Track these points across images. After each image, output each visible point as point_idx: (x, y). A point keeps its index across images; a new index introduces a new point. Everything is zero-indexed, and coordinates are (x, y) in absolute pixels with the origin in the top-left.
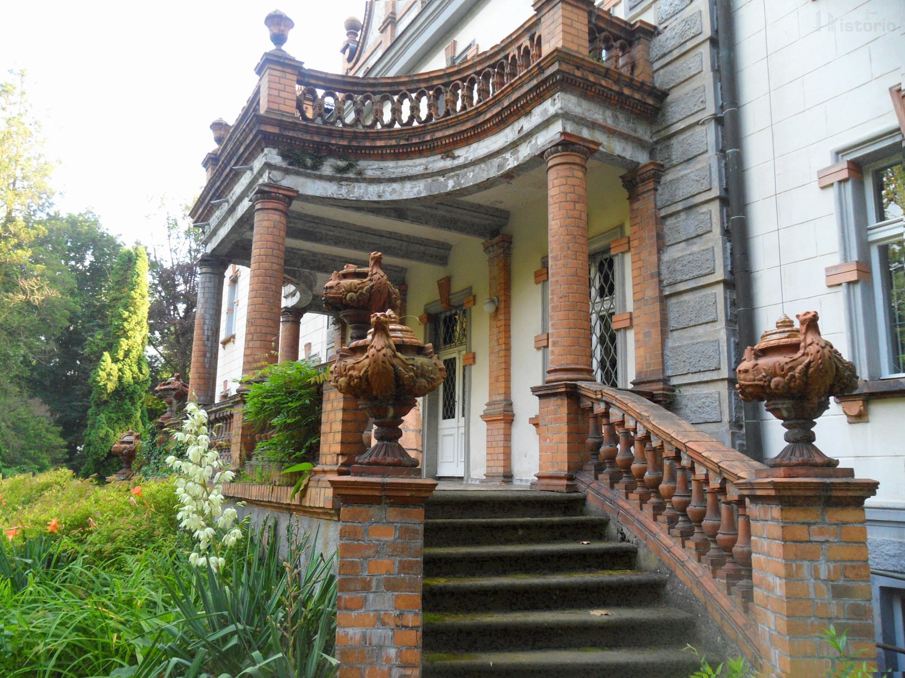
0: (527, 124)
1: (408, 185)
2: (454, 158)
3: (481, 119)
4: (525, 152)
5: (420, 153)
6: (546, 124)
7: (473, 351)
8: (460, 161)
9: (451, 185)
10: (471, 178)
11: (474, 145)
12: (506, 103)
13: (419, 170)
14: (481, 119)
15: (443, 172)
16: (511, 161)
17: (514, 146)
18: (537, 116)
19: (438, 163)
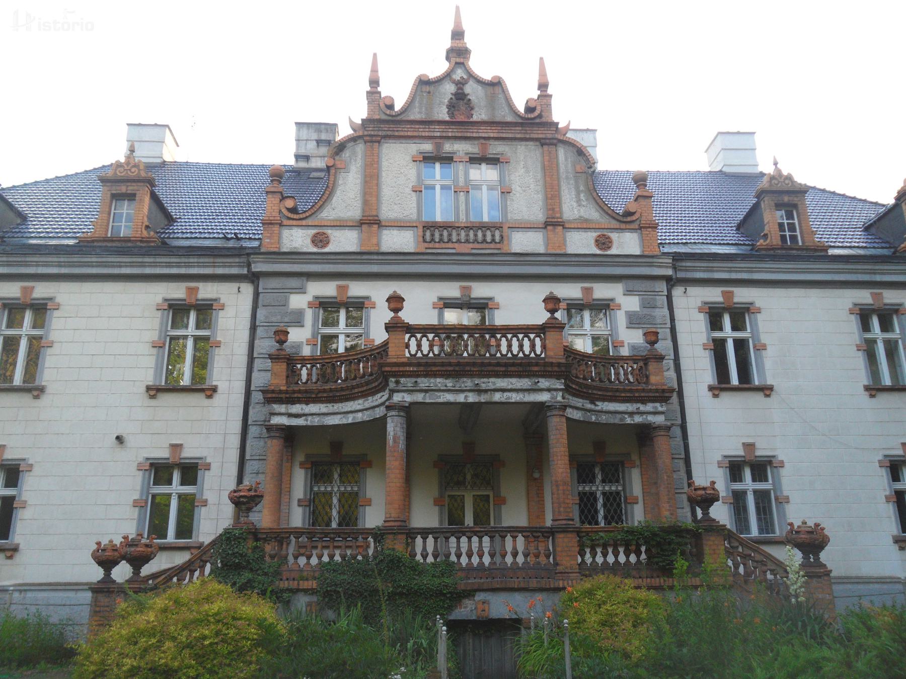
0: (642, 408)
1: (575, 411)
2: (596, 405)
3: (617, 394)
4: (638, 419)
5: (582, 397)
6: (655, 413)
7: (502, 495)
8: (598, 408)
9: (594, 418)
10: (604, 419)
11: (606, 403)
12: (637, 395)
13: (579, 405)
14: (617, 394)
15: (590, 411)
16: (628, 420)
17: (631, 414)
18: (649, 407)
19: (589, 406)
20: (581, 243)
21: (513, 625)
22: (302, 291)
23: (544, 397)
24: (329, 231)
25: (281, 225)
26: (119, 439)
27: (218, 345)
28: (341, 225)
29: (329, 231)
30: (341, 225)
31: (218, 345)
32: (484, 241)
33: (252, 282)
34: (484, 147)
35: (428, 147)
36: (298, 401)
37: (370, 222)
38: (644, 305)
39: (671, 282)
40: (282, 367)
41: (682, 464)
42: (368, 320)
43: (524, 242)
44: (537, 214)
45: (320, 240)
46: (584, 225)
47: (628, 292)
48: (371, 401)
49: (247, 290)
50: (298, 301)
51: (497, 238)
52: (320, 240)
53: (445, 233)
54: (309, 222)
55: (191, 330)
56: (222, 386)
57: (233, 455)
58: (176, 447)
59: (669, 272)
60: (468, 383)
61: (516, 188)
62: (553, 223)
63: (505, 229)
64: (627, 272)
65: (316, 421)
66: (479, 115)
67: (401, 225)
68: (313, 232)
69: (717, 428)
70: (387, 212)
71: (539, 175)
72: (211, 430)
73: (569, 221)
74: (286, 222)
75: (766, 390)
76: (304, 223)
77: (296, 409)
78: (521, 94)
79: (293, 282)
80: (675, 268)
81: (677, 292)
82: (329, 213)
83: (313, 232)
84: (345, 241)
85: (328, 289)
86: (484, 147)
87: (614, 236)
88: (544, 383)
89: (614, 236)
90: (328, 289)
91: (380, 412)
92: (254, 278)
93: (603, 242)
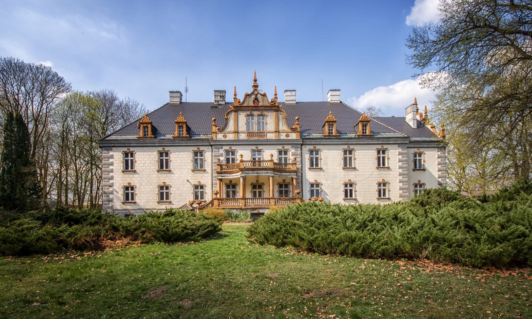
20: (283, 136)
21: (263, 214)
22: (222, 148)
23: (270, 174)
27: (205, 161)
31: (205, 161)
35: (248, 113)
37: (237, 132)
39: (302, 145)
40: (219, 167)
41: (301, 184)
43: (271, 136)
44: (273, 129)
45: (225, 136)
47: (292, 147)
48: (237, 174)
49: (210, 147)
52: (225, 136)
55: (199, 157)
56: (207, 169)
57: (210, 183)
60: (255, 172)
62: (277, 132)
64: (293, 144)
66: (261, 104)
69: (310, 176)
71: (274, 119)
75: (321, 169)
78: (270, 97)
79: (220, 146)
80: (303, 142)
81: (303, 147)
85: (227, 148)
87: (290, 134)
88: (269, 172)
90: (227, 148)
91: (239, 176)
92: (211, 146)
93: (287, 136)
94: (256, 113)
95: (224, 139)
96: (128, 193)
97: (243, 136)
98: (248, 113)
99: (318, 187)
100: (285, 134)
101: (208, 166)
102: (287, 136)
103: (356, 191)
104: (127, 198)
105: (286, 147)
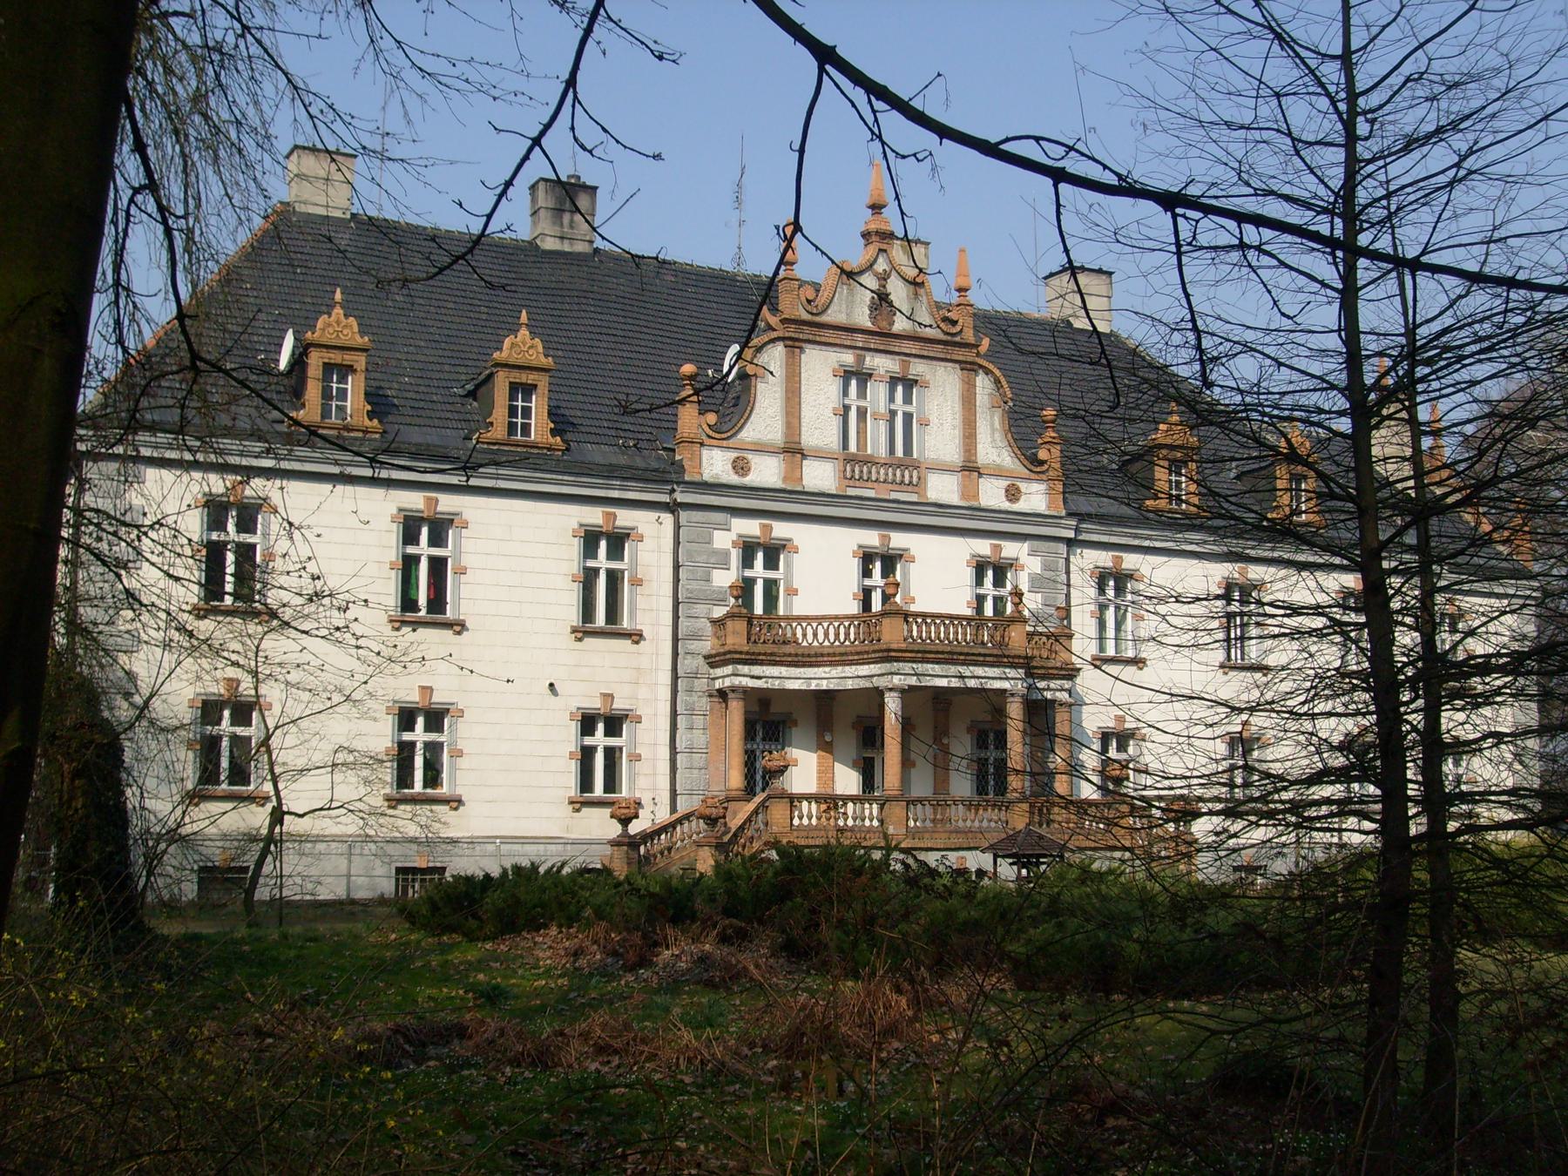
20: (992, 494)
24: (750, 456)
25: (702, 444)
26: (551, 685)
28: (761, 449)
29: (750, 456)
30: (761, 449)
32: (902, 482)
33: (673, 512)
34: (905, 365)
36: (762, 663)
37: (793, 451)
38: (1046, 567)
42: (788, 565)
43: (943, 489)
45: (741, 467)
46: (998, 473)
49: (667, 518)
50: (723, 540)
51: (915, 480)
52: (741, 467)
53: (865, 469)
54: (731, 443)
57: (665, 708)
58: (609, 697)
59: (1071, 534)
61: (933, 419)
63: (923, 470)
65: (777, 684)
67: (821, 455)
68: (734, 455)
69: (1098, 700)
70: (809, 439)
72: (638, 676)
73: (987, 466)
74: (707, 441)
76: (725, 443)
77: (757, 670)
80: (1077, 530)
82: (749, 434)
83: (734, 455)
84: (767, 472)
86: (905, 365)
89: (1023, 486)
90: (750, 527)
93: (1013, 494)
94: (882, 364)
95: (734, 479)
96: (413, 744)
97: (820, 476)
98: (848, 358)
99: (440, 729)
100: (1005, 483)
101: (650, 607)
102: (1013, 494)
103: (638, 758)
104: (404, 778)
105: (1010, 549)
